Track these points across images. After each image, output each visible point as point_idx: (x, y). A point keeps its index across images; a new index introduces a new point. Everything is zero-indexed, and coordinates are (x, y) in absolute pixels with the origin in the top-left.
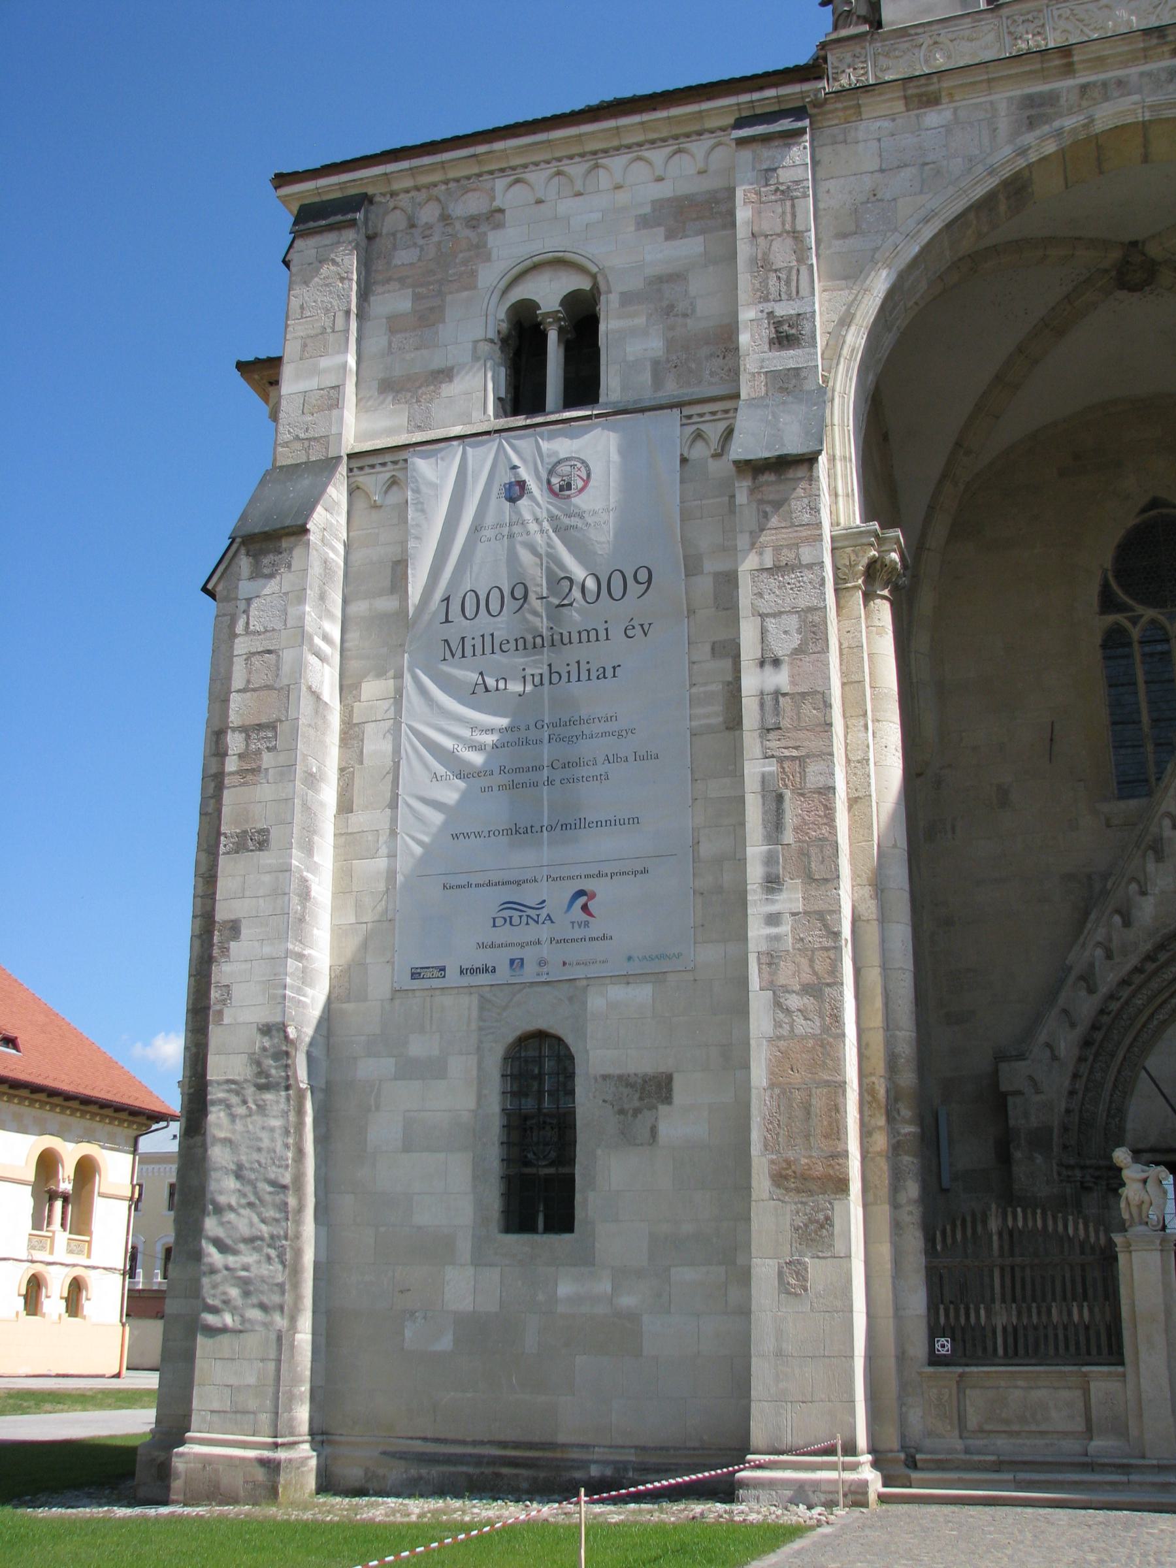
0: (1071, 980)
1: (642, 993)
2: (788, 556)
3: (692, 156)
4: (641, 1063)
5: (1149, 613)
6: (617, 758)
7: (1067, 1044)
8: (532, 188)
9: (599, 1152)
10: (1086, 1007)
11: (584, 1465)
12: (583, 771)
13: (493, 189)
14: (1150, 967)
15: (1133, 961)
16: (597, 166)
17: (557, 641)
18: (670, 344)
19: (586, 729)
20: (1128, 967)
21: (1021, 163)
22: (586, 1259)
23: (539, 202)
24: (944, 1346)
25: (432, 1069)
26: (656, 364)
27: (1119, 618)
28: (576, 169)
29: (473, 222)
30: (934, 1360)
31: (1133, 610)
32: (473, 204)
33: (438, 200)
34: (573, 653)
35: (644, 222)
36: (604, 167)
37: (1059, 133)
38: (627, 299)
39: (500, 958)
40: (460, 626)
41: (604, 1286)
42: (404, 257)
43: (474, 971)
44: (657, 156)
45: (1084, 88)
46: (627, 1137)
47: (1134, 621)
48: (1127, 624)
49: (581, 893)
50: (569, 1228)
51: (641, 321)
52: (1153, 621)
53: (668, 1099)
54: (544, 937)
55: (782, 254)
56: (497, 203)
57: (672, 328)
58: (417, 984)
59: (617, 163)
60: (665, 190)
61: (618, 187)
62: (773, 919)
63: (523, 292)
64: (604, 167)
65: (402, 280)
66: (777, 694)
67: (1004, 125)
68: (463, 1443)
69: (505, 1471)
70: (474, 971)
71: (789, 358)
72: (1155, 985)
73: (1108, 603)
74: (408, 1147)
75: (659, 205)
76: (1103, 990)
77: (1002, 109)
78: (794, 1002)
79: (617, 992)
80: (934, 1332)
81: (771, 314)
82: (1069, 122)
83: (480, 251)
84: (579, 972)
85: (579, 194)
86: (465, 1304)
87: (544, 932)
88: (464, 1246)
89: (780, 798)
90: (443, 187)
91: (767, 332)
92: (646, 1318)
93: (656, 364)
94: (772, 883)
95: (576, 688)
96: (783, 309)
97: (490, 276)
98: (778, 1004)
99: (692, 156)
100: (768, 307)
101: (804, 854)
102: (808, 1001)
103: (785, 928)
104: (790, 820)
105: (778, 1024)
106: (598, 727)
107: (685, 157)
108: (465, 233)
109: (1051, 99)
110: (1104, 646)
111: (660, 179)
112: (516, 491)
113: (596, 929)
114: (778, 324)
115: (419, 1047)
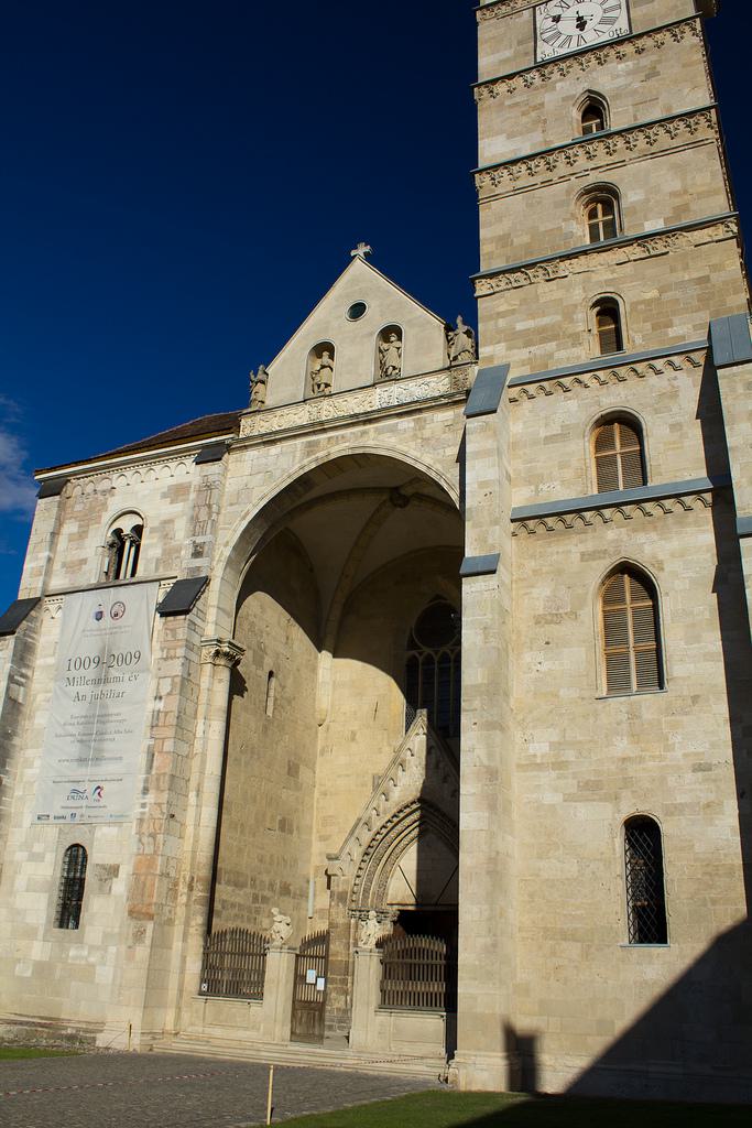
0: (361, 824)
1: (114, 830)
2: (172, 653)
4: (110, 861)
5: (427, 650)
6: (119, 732)
7: (357, 853)
9: (91, 896)
10: (366, 837)
11: (66, 1028)
12: (107, 737)
14: (396, 820)
15: (388, 817)
17: (106, 681)
18: (164, 551)
19: (110, 719)
20: (386, 819)
21: (302, 472)
22: (80, 941)
24: (205, 987)
25: (36, 858)
26: (157, 560)
27: (414, 652)
29: (104, 492)
30: (201, 993)
31: (420, 648)
32: (105, 485)
34: (110, 686)
35: (164, 496)
37: (317, 459)
38: (153, 530)
39: (67, 813)
40: (73, 673)
41: (85, 953)
42: (78, 507)
43: (59, 818)
45: (329, 438)
46: (101, 889)
47: (421, 654)
48: (417, 655)
49: (99, 787)
50: (77, 927)
51: (155, 540)
52: (429, 655)
53: (117, 876)
54: (84, 805)
55: (203, 516)
57: (165, 544)
58: (39, 822)
60: (172, 481)
62: (143, 806)
63: (116, 526)
65: (75, 518)
66: (159, 711)
67: (298, 454)
68: (28, 1016)
69: (40, 1029)
70: (59, 818)
71: (198, 562)
72: (399, 827)
73: (412, 645)
74: (27, 891)
75: (170, 488)
76: (375, 830)
77: (299, 446)
78: (145, 840)
79: (105, 829)
80: (203, 980)
81: (194, 542)
82: (320, 454)
83: (104, 505)
84: (94, 820)
86: (38, 959)
87: (84, 803)
88: (40, 937)
89: (153, 755)
91: (191, 550)
92: (98, 968)
93: (157, 560)
94: (146, 791)
95: (108, 701)
96: (199, 540)
97: (107, 517)
98: (140, 840)
100: (194, 538)
101: (158, 780)
102: (151, 839)
103: (147, 810)
104: (155, 764)
105: (139, 849)
106: (114, 718)
108: (102, 498)
109: (318, 442)
110: (407, 666)
112: (99, 616)
113: (103, 802)
114: (196, 545)
115: (37, 848)
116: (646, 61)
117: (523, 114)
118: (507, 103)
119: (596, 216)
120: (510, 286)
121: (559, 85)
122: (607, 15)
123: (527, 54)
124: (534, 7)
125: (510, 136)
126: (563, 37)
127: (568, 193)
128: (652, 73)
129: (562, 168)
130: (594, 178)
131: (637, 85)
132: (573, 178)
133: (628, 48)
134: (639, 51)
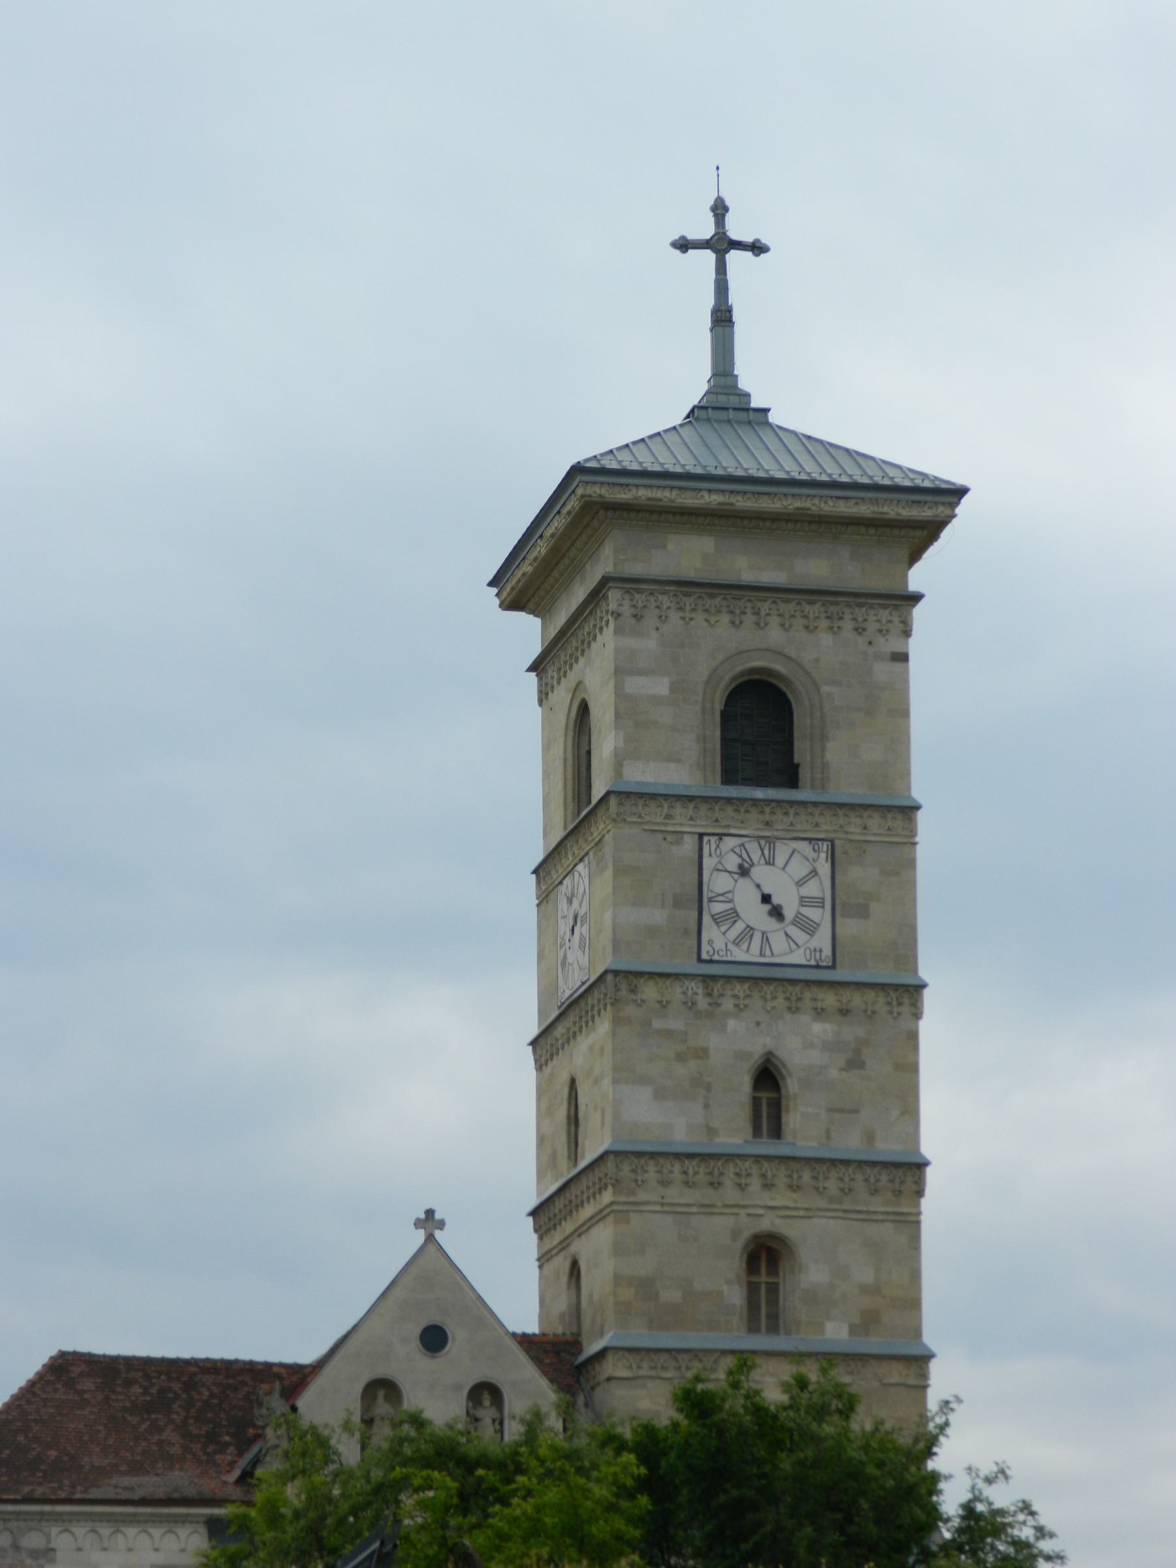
3: (178, 1536)
8: (76, 1540)
13: (50, 1534)
16: (118, 1531)
23: (79, 1549)
28: (105, 1531)
29: (35, 1554)
32: (33, 1540)
33: (12, 1533)
36: (121, 1532)
44: (156, 1532)
56: (52, 1545)
59: (131, 1531)
61: (130, 1550)
64: (121, 1532)
85: (105, 1549)
90: (16, 1524)
99: (178, 1536)
107: (173, 1537)
111: (156, 1550)
116: (853, 1031)
117: (681, 1058)
118: (657, 1024)
119: (758, 1273)
120: (653, 1373)
121: (732, 1023)
122: (805, 910)
123: (686, 932)
124: (701, 836)
125: (660, 1094)
126: (739, 926)
127: (735, 1234)
128: (855, 1063)
129: (730, 1193)
130: (767, 1223)
131: (834, 1073)
132: (743, 1212)
133: (829, 999)
134: (845, 1012)
